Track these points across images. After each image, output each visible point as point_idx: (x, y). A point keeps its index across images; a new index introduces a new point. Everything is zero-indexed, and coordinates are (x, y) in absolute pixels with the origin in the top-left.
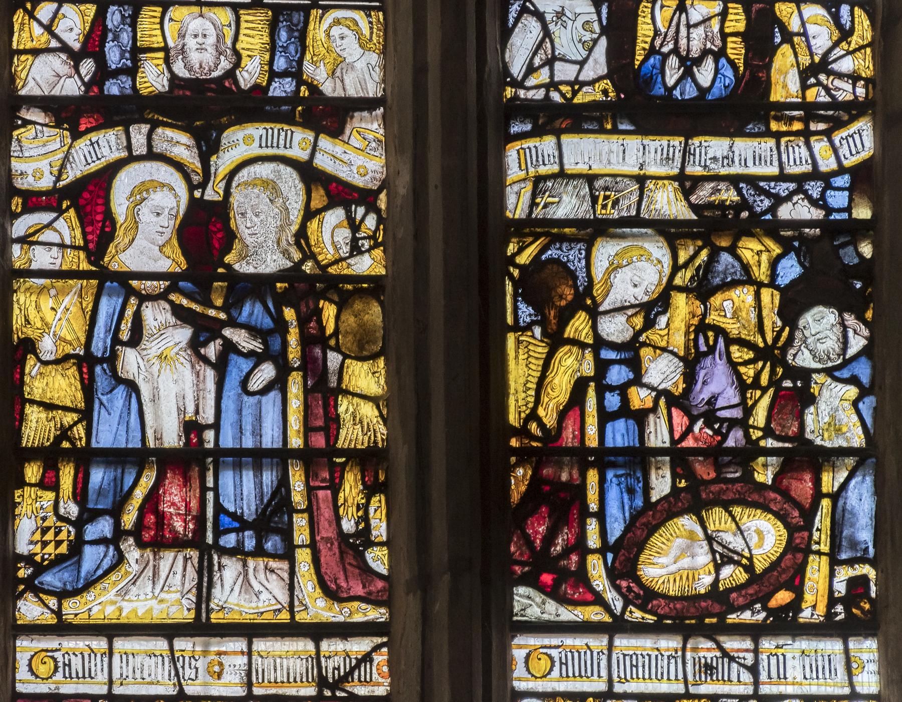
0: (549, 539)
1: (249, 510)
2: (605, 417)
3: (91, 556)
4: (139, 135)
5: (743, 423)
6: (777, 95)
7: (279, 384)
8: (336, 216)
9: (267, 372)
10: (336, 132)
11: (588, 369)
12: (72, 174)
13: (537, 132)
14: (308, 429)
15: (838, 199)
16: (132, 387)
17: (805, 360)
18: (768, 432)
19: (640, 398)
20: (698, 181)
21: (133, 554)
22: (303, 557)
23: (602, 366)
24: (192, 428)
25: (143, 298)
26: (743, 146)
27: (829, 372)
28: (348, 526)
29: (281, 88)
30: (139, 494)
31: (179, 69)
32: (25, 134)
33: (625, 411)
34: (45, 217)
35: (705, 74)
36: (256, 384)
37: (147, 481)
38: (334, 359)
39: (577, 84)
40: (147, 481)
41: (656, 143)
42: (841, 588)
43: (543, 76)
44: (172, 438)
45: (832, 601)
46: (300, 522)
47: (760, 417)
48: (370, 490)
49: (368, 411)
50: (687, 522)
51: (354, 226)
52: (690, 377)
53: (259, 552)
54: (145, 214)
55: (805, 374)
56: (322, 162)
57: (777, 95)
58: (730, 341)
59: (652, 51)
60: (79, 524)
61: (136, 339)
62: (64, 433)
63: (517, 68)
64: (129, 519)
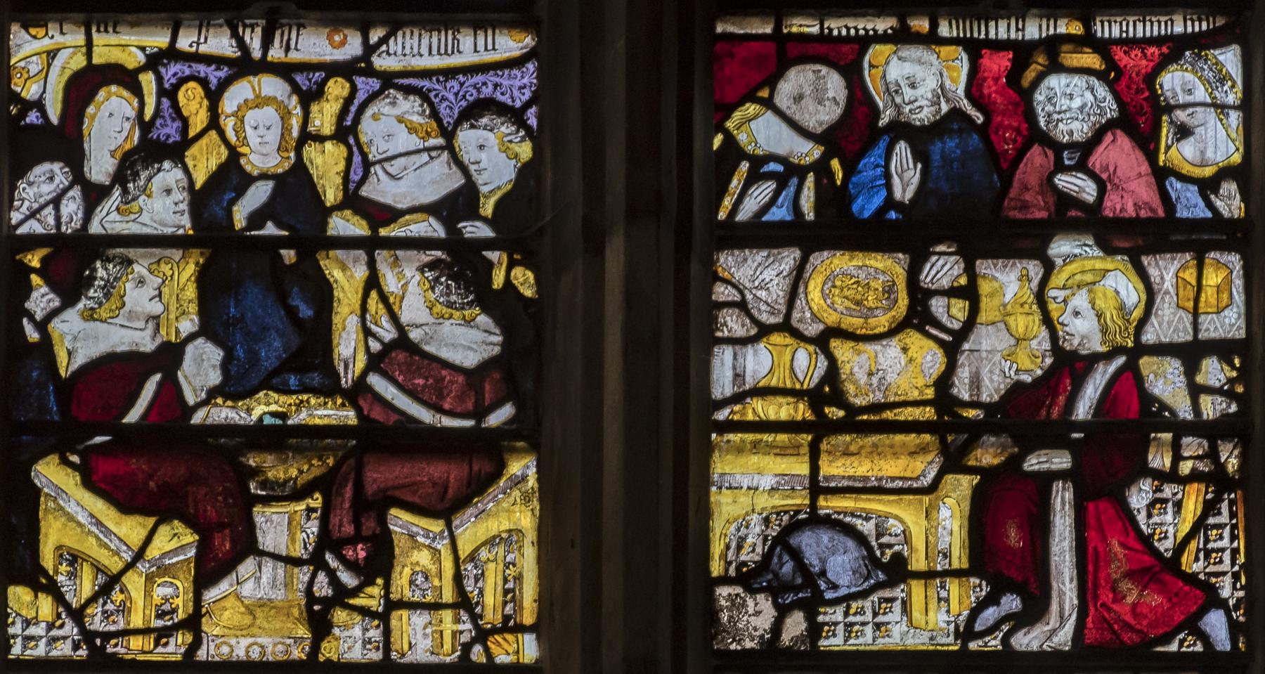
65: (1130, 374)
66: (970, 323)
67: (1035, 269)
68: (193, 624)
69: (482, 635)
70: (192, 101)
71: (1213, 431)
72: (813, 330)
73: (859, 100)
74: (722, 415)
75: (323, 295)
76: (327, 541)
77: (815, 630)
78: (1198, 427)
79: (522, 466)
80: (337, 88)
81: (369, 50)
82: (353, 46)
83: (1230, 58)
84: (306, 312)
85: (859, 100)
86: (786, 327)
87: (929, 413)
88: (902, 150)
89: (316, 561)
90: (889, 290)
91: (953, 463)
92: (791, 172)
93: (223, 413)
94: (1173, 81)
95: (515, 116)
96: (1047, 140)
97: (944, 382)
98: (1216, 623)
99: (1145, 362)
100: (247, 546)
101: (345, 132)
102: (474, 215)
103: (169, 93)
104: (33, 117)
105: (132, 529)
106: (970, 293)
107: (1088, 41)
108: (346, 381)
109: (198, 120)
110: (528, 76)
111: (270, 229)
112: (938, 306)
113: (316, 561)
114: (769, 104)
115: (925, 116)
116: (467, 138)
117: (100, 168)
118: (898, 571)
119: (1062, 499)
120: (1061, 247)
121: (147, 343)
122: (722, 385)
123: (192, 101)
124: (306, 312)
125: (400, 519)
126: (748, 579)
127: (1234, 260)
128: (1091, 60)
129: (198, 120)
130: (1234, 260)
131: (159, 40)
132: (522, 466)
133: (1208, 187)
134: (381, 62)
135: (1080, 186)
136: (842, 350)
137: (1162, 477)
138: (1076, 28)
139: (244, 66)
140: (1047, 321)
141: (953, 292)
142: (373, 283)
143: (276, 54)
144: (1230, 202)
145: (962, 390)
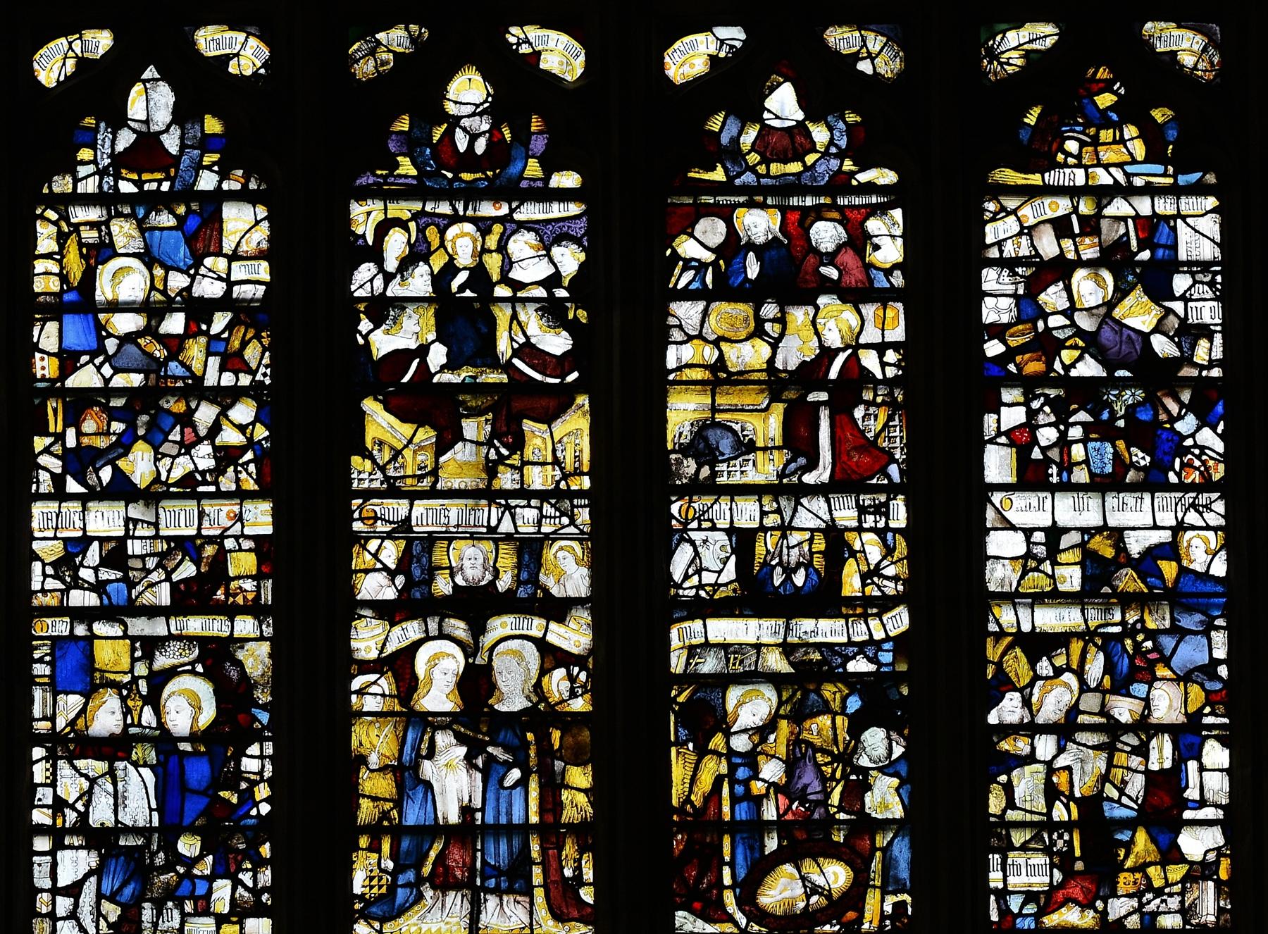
0: (699, 880)
1: (504, 861)
2: (735, 800)
3: (401, 894)
4: (433, 625)
5: (824, 803)
6: (846, 592)
7: (523, 783)
8: (560, 673)
9: (515, 774)
10: (561, 620)
11: (724, 769)
12: (390, 649)
13: (691, 617)
14: (542, 811)
15: (886, 657)
16: (428, 786)
17: (864, 762)
18: (841, 809)
19: (758, 787)
20: (795, 647)
21: (429, 893)
22: (539, 894)
23: (733, 768)
24: (466, 811)
25: (436, 728)
26: (825, 624)
27: (880, 769)
28: (568, 873)
29: (522, 593)
30: (433, 854)
31: (459, 580)
32: (359, 624)
33: (748, 795)
34: (372, 677)
35: (799, 579)
36: (508, 782)
37: (437, 847)
38: (559, 765)
39: (716, 586)
40: (437, 847)
41: (767, 623)
42: (888, 909)
43: (695, 580)
44: (454, 818)
45: (883, 917)
46: (537, 871)
47: (835, 798)
48: (581, 852)
49: (582, 799)
50: (788, 868)
51: (572, 678)
52: (790, 772)
53: (510, 891)
54: (437, 673)
55: (865, 771)
56: (551, 638)
57: (846, 592)
58: (816, 749)
59: (765, 564)
60: (394, 874)
61: (431, 755)
62: (385, 815)
63: (677, 576)
64: (426, 870)
65: (854, 358)
66: (782, 335)
67: (811, 310)
68: (434, 473)
69: (565, 477)
70: (432, 234)
71: (890, 383)
72: (712, 337)
73: (732, 231)
74: (671, 377)
75: (492, 323)
76: (494, 435)
77: (714, 474)
78: (885, 381)
79: (583, 400)
80: (497, 229)
81: (512, 211)
82: (504, 210)
83: (897, 214)
84: (484, 330)
85: (732, 231)
86: (700, 336)
87: (763, 376)
88: (751, 255)
89: (489, 444)
90: (746, 319)
91: (775, 398)
92: (701, 267)
93: (447, 377)
94: (873, 225)
95: (577, 241)
96: (816, 251)
97: (771, 361)
98: (894, 470)
99: (861, 353)
100: (459, 437)
101: (502, 248)
102: (560, 286)
103: (422, 231)
104: (360, 242)
105: (407, 429)
106: (782, 320)
107: (834, 206)
108: (503, 361)
109: (435, 243)
110: (583, 223)
111: (468, 293)
112: (768, 326)
113: (489, 444)
114: (692, 235)
115: (761, 240)
116: (556, 251)
117: (391, 265)
118: (751, 447)
119: (824, 415)
120: (822, 300)
121: (413, 345)
122: (671, 363)
123: (432, 234)
124: (484, 330)
125: (528, 425)
126: (685, 450)
127: (900, 306)
128: (836, 215)
129: (435, 243)
130: (900, 306)
131: (417, 206)
132: (583, 400)
133: (888, 272)
134: (517, 216)
135: (832, 273)
136: (724, 346)
137: (869, 404)
138: (828, 200)
139: (455, 219)
140: (817, 333)
141: (774, 320)
142: (514, 317)
143: (470, 213)
144: (898, 280)
145: (779, 365)
